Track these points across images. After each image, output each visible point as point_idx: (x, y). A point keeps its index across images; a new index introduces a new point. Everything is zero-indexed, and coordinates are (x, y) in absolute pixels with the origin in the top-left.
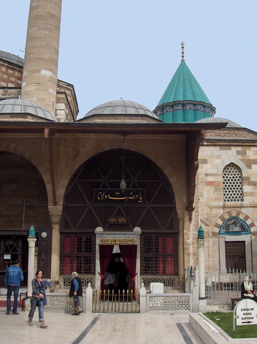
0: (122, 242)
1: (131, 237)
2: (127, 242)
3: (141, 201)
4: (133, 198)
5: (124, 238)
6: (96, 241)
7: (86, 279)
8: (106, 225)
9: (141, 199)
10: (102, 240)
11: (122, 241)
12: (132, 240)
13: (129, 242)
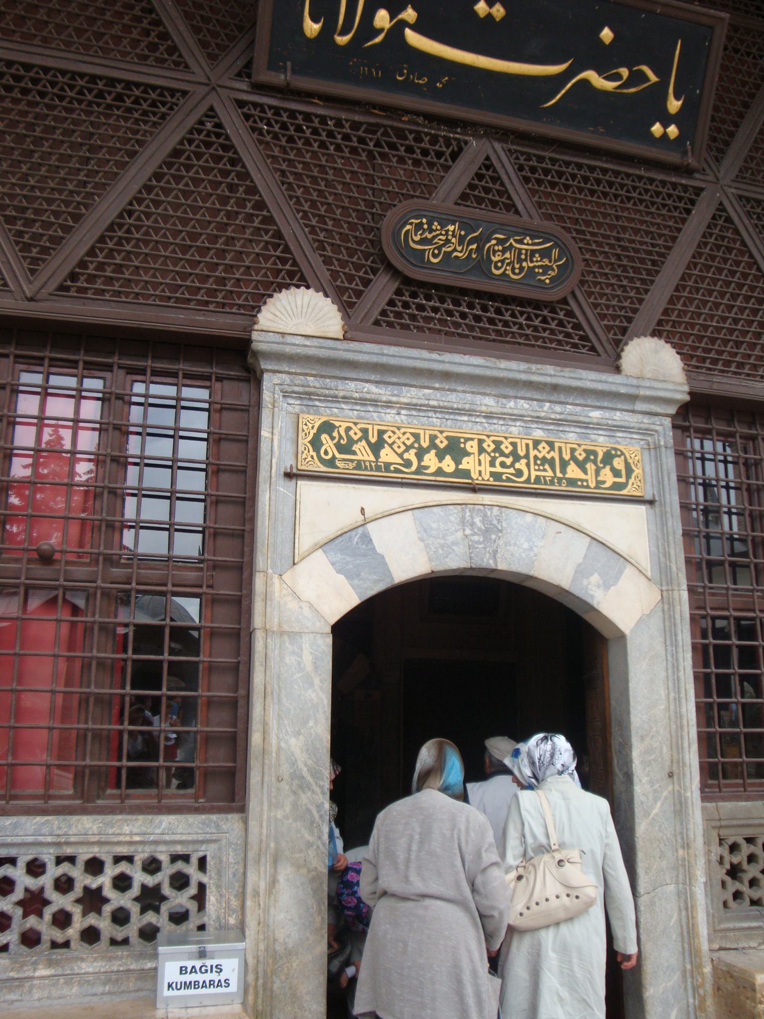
0: (521, 465)
1: (598, 426)
2: (564, 465)
3: (673, 130)
4: (610, 85)
5: (538, 434)
6: (265, 433)
7: (130, 859)
8: (366, 283)
9: (674, 105)
10: (327, 428)
11: (517, 458)
12: (608, 458)
13: (581, 465)
